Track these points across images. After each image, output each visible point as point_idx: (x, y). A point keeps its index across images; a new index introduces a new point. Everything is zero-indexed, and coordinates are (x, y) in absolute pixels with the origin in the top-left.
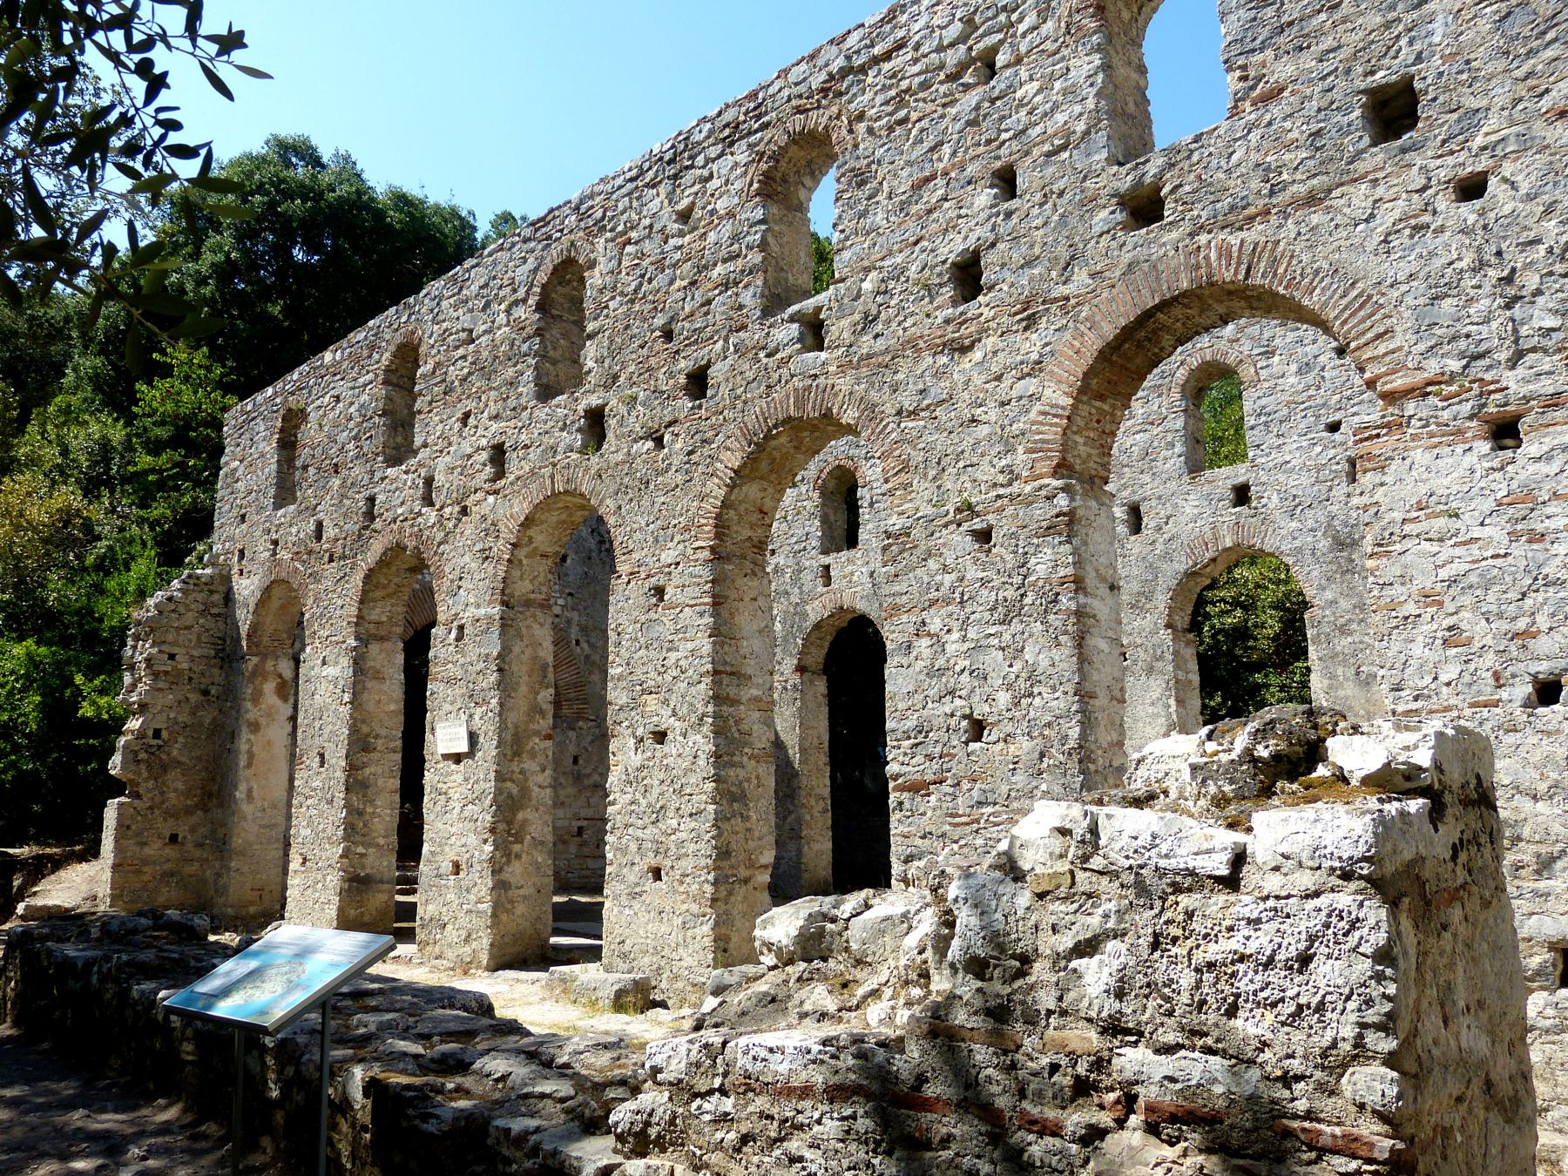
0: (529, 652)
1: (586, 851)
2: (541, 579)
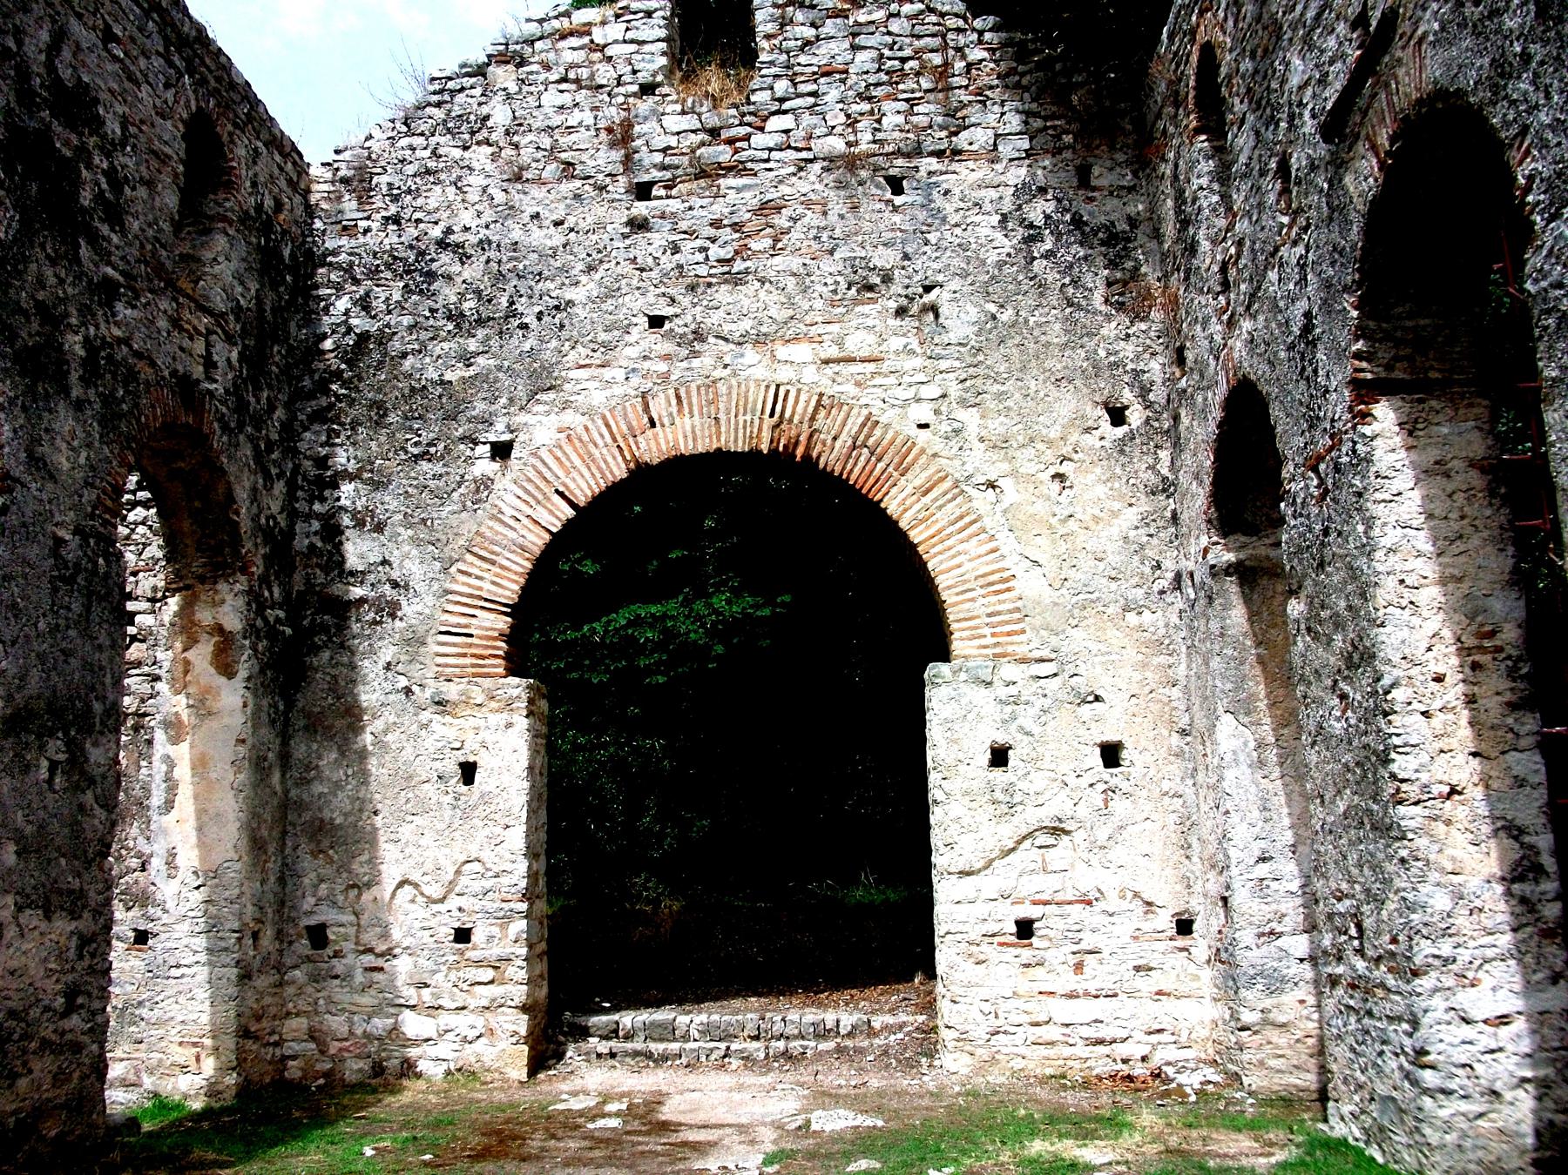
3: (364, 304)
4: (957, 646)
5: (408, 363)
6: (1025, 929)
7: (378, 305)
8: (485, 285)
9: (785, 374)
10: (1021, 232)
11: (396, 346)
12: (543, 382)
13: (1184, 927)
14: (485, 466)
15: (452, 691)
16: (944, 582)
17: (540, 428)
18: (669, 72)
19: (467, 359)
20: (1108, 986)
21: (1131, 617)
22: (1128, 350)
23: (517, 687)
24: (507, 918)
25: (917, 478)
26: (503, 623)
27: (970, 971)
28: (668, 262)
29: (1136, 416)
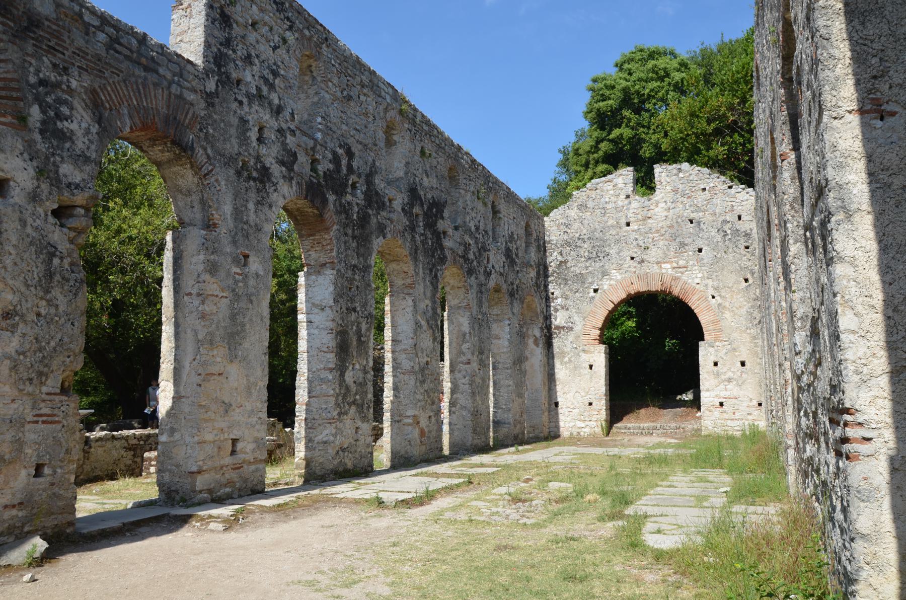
0: (457, 329)
1: (725, 416)
2: (462, 297)
3: (561, 253)
4: (706, 337)
5: (572, 269)
6: (721, 404)
7: (564, 254)
8: (590, 249)
9: (664, 271)
10: (723, 234)
11: (569, 264)
12: (605, 273)
13: (760, 405)
14: (592, 294)
15: (586, 348)
16: (702, 322)
17: (605, 285)
18: (633, 191)
19: (587, 268)
20: (741, 417)
21: (748, 331)
22: (750, 263)
23: (602, 348)
24: (601, 399)
25: (695, 297)
26: (598, 332)
27: (708, 413)
28: (635, 243)
29: (750, 281)
